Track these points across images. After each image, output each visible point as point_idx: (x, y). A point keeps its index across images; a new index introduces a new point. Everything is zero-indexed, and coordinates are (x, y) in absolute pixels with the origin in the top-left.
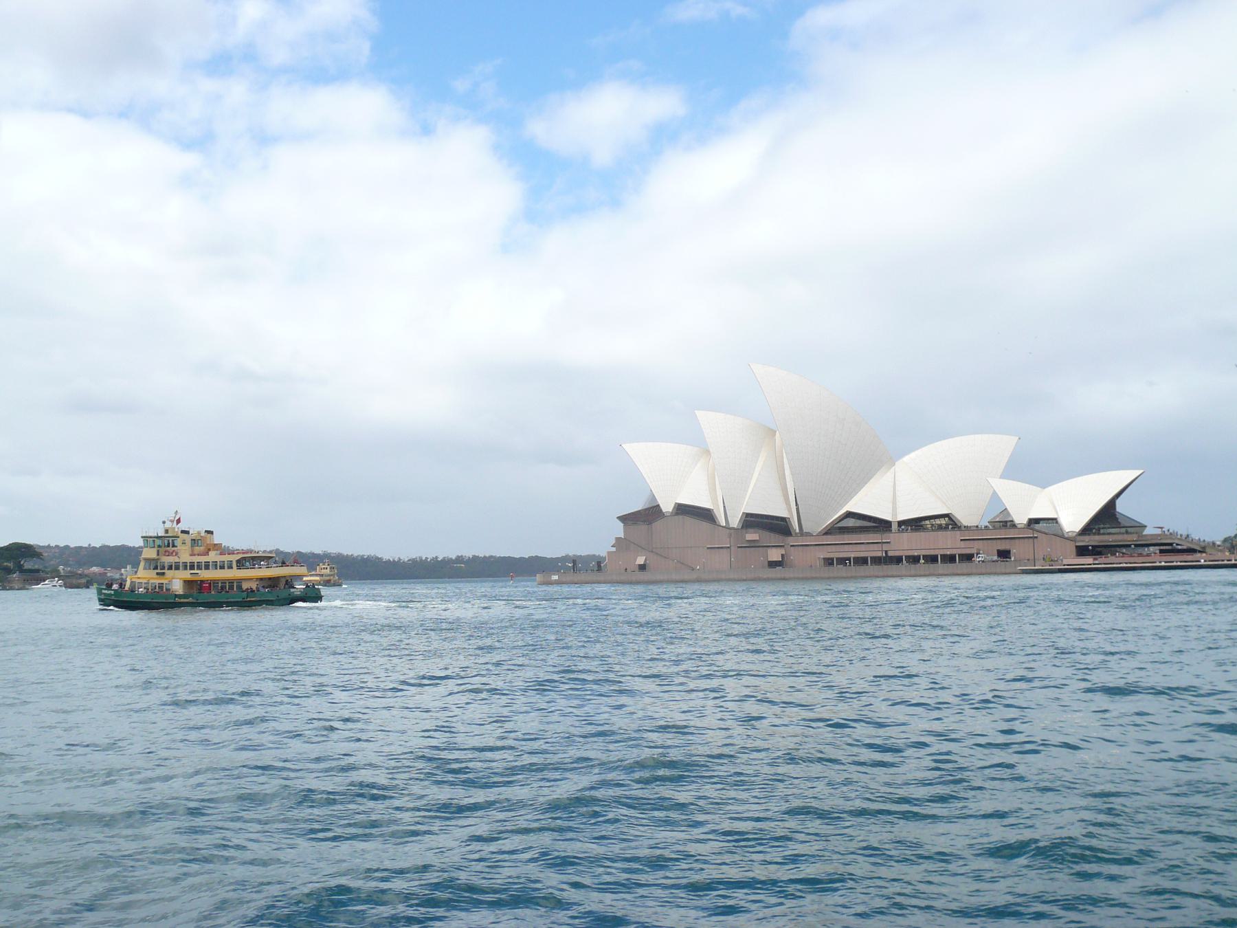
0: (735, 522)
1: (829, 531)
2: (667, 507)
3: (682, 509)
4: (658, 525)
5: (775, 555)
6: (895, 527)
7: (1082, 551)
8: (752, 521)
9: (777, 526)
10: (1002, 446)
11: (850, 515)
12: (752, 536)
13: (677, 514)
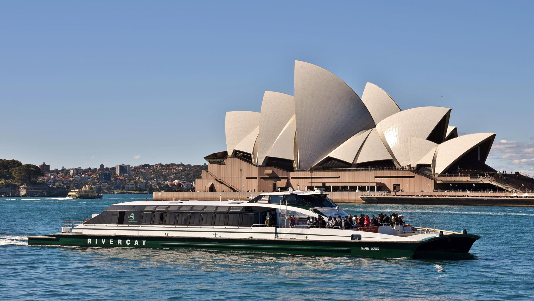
0: (261, 163)
3: (236, 153)
5: (282, 183)
7: (439, 187)
8: (270, 162)
9: (286, 165)
12: (269, 171)
13: (233, 157)
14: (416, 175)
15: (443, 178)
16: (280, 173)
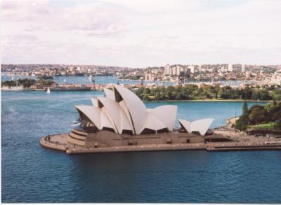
0: (120, 132)
2: (100, 128)
4: (98, 134)
5: (131, 141)
8: (125, 132)
11: (146, 129)
12: (126, 136)
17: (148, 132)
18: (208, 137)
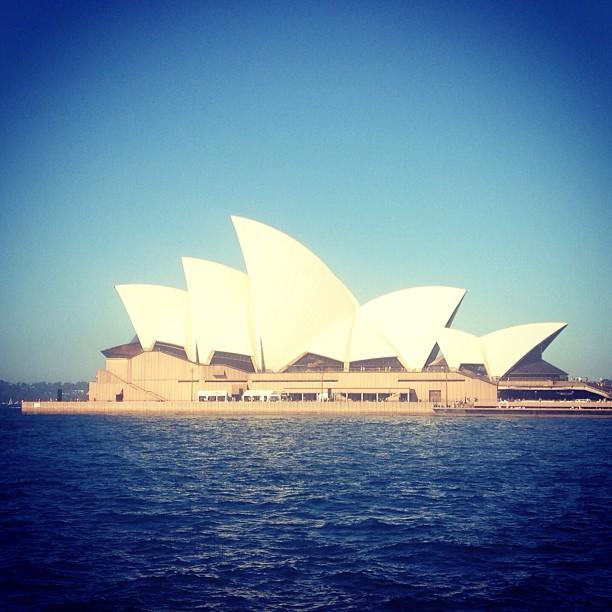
0: (205, 358)
1: (288, 370)
2: (147, 343)
3: (160, 347)
6: (347, 366)
8: (220, 358)
10: (448, 297)
11: (308, 354)
12: (219, 369)
14: (466, 378)
15: (508, 383)
16: (233, 373)
17: (309, 362)
18: (505, 386)
